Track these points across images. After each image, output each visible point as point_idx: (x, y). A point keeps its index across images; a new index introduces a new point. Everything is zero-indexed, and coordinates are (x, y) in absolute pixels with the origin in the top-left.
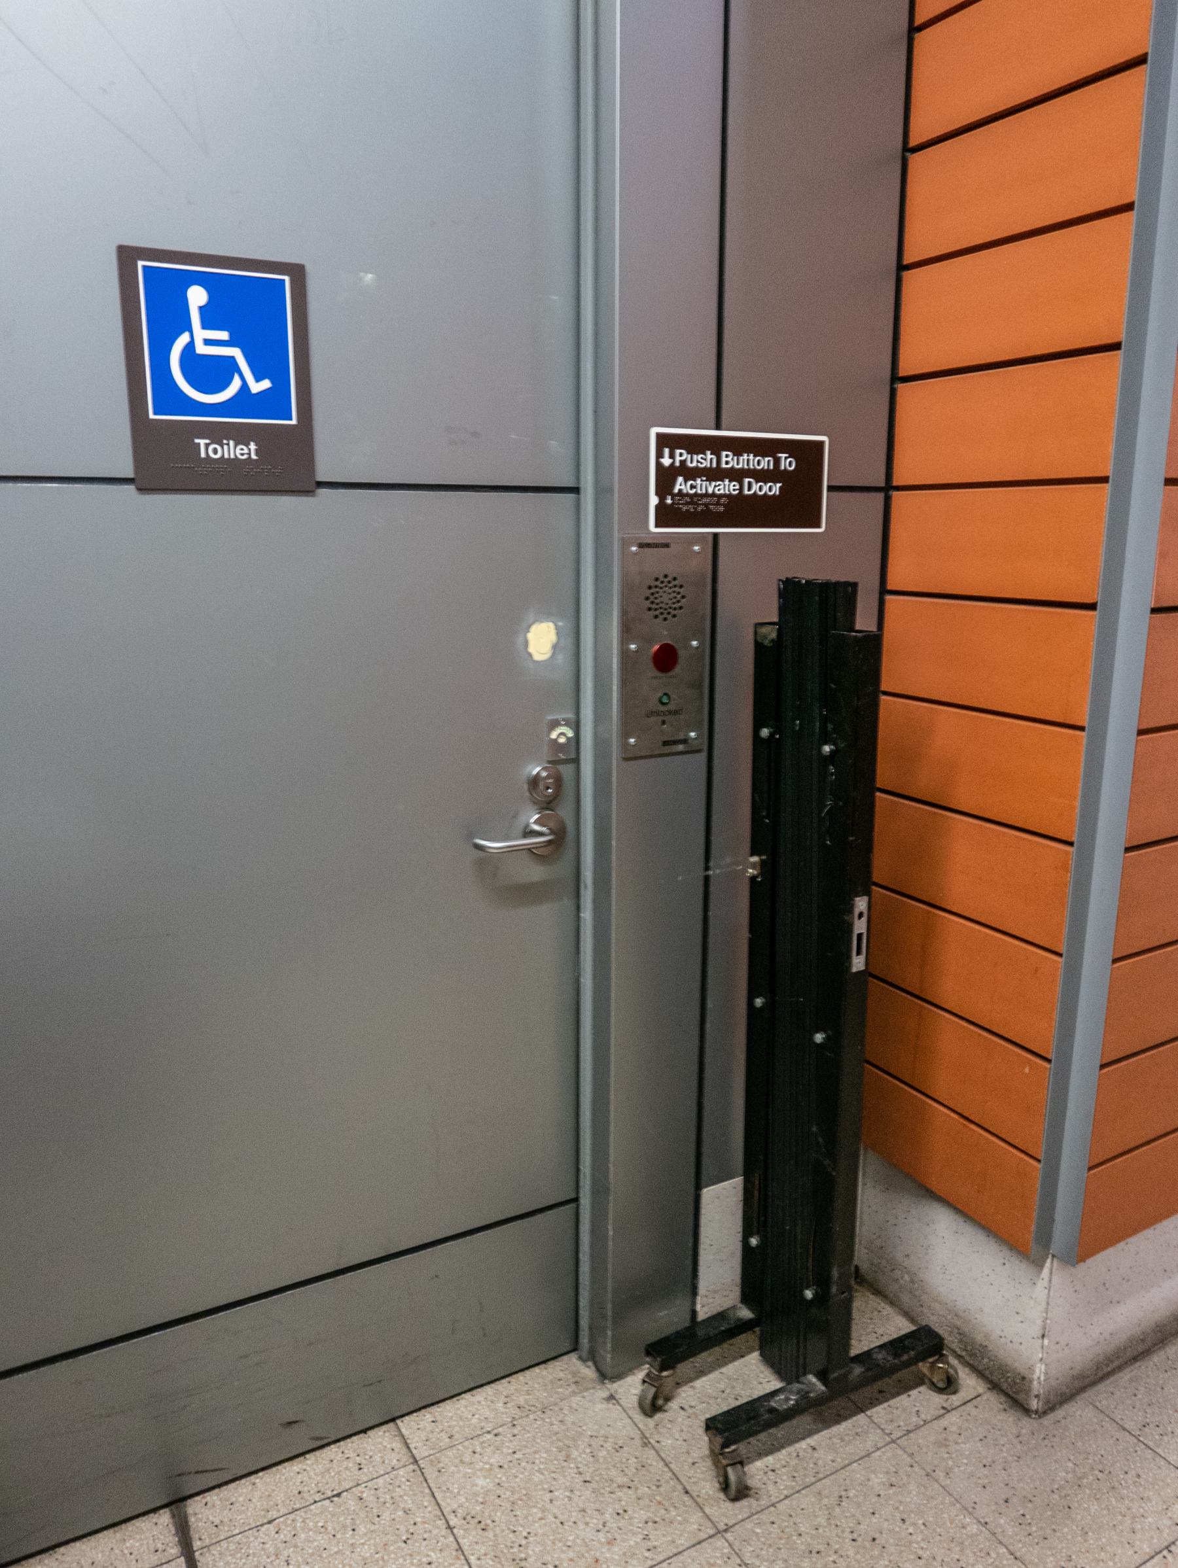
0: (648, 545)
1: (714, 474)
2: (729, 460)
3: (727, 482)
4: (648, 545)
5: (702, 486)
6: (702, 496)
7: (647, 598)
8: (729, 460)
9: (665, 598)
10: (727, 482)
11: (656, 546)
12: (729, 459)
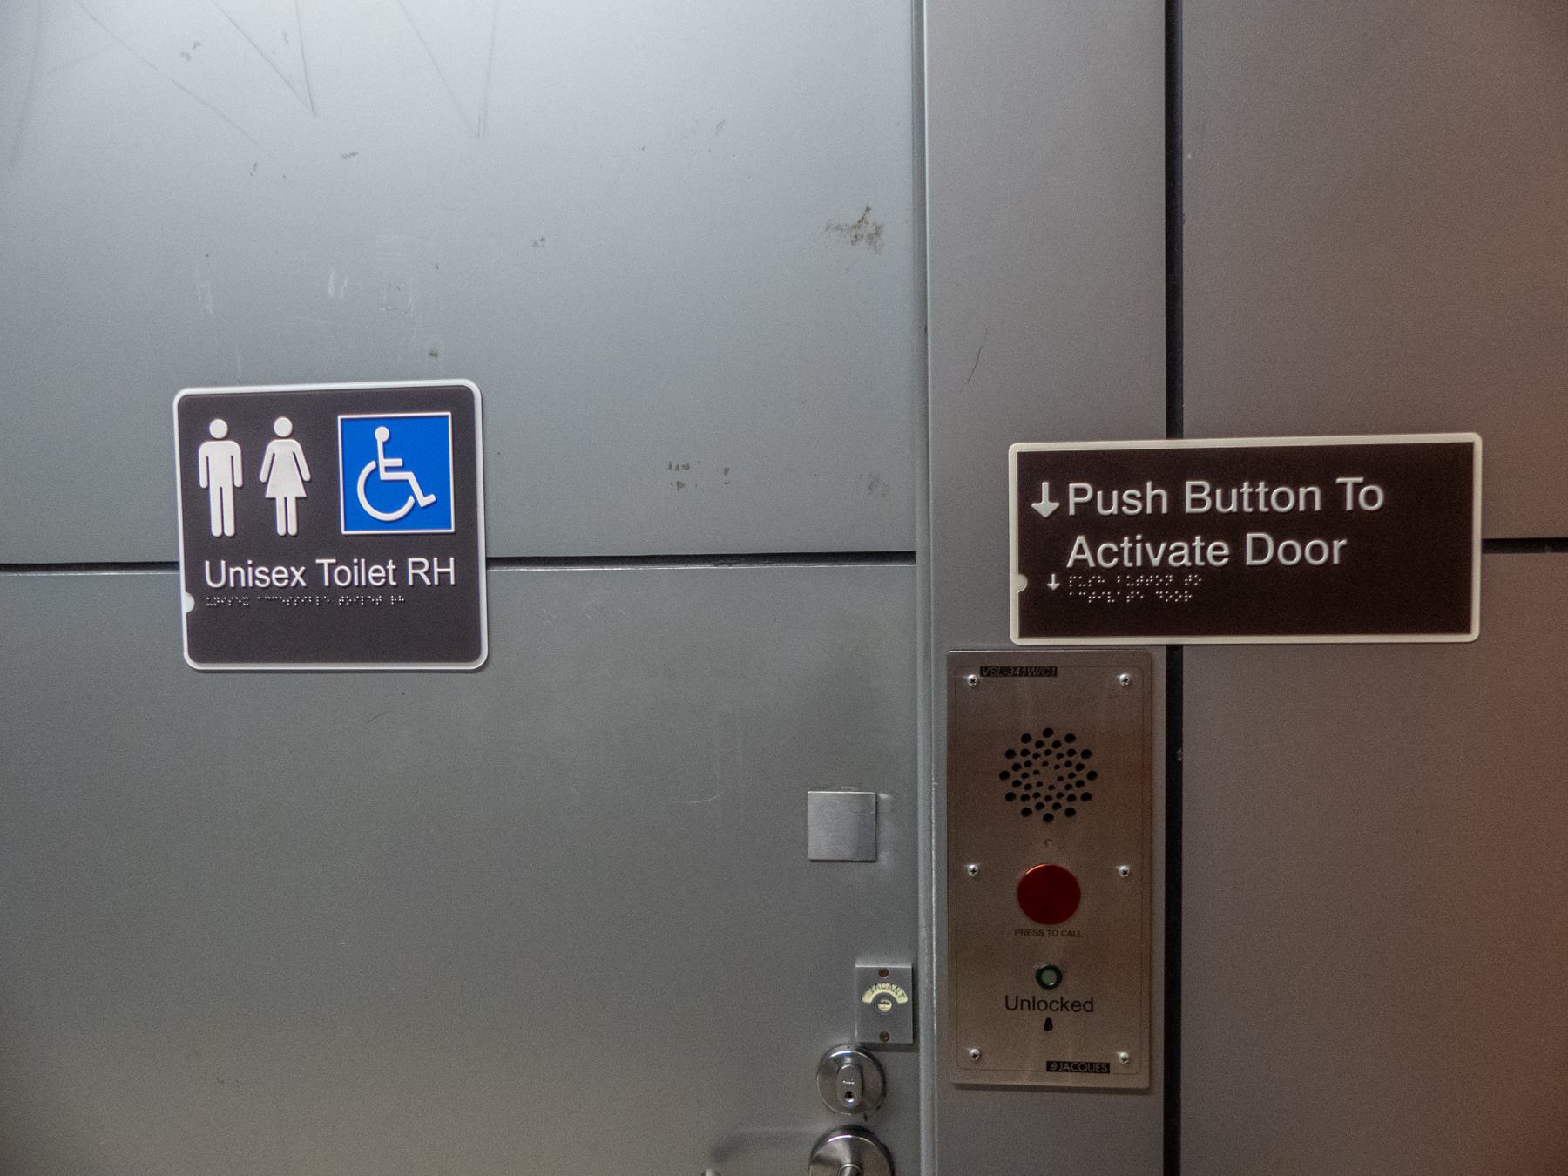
0: (1005, 671)
1: (1169, 525)
2: (1199, 496)
3: (1198, 542)
4: (1005, 671)
6: (1135, 572)
7: (1004, 775)
9: (1049, 776)
10: (1198, 542)
11: (1025, 672)
12: (1204, 495)
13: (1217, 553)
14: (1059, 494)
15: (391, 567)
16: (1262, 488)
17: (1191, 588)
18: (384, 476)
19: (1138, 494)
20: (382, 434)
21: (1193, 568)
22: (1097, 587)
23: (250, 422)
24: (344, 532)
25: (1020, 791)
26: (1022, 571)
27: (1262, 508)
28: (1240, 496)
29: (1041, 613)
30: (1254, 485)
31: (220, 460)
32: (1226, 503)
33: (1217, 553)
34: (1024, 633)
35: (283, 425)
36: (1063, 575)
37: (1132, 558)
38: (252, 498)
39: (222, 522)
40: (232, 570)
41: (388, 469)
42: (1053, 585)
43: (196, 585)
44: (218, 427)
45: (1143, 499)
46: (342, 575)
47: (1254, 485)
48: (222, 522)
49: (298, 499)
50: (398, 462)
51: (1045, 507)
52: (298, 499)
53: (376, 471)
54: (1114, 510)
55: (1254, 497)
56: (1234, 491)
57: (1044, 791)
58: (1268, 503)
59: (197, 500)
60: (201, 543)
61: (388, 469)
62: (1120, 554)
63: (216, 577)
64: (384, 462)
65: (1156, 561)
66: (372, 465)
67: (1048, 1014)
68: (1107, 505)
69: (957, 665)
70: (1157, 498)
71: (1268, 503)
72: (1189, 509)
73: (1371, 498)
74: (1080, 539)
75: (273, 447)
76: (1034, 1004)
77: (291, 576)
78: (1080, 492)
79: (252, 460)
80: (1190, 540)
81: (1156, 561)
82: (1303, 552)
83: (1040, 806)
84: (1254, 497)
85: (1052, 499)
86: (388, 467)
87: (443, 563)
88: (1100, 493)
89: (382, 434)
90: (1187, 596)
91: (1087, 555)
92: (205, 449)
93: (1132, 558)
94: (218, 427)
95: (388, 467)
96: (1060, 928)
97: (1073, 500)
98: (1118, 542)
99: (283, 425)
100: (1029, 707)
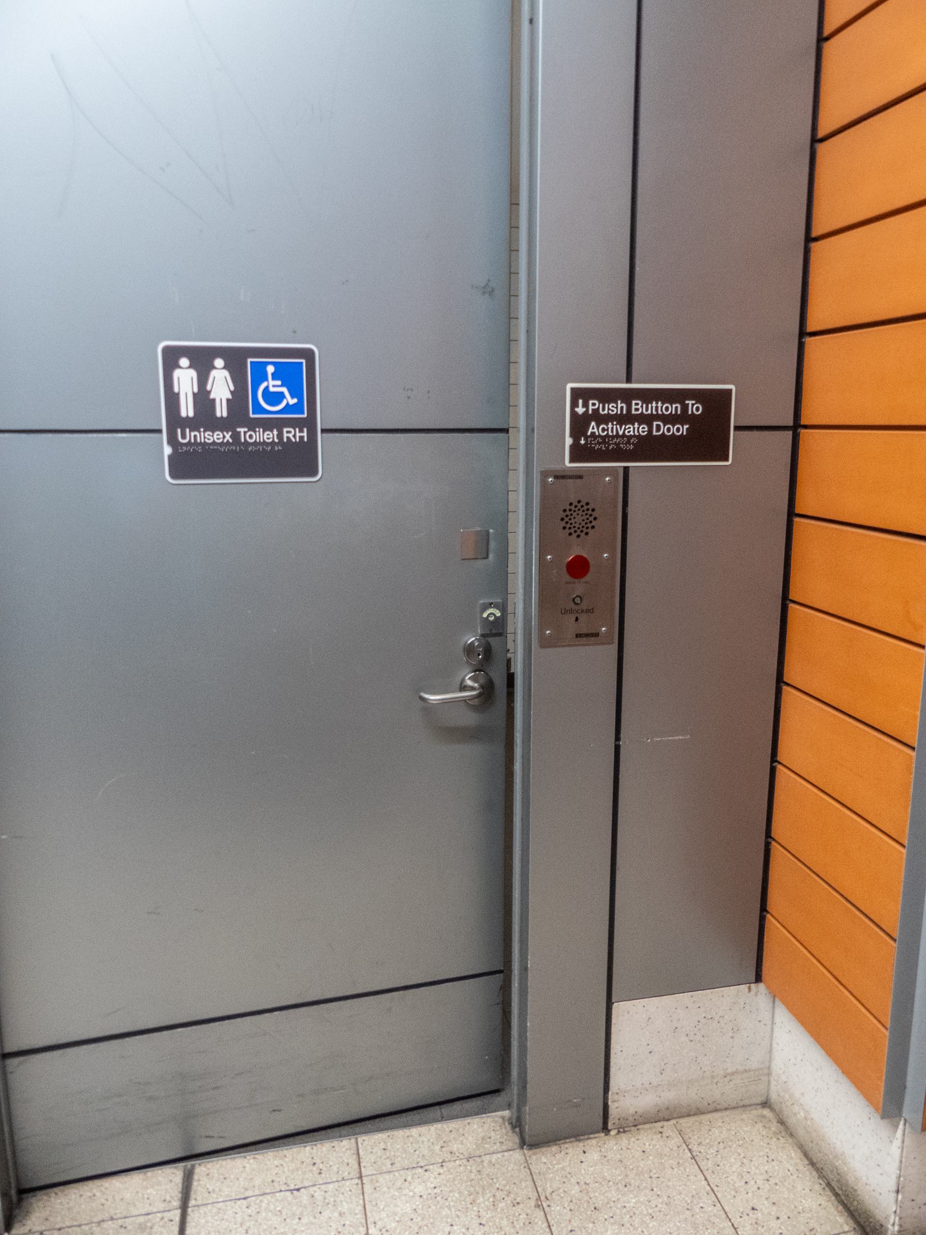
0: (563, 477)
1: (626, 419)
2: (638, 407)
3: (636, 425)
4: (563, 477)
5: (612, 428)
6: (613, 437)
7: (562, 519)
8: (638, 407)
9: (579, 519)
10: (636, 425)
11: (571, 477)
12: (639, 407)
13: (643, 430)
14: (585, 405)
15: (275, 432)
16: (660, 404)
17: (633, 444)
18: (272, 389)
20: (270, 369)
21: (635, 436)
22: (599, 443)
23: (202, 360)
24: (251, 416)
25: (568, 526)
26: (571, 436)
27: (660, 412)
29: (578, 453)
30: (657, 403)
31: (185, 379)
32: (647, 410)
33: (643, 430)
34: (572, 461)
35: (219, 363)
36: (586, 438)
37: (612, 431)
38: (203, 398)
39: (187, 409)
40: (193, 434)
41: (274, 386)
42: (583, 442)
43: (172, 441)
44: (184, 362)
45: (617, 408)
46: (251, 437)
47: (657, 403)
48: (187, 409)
49: (228, 400)
50: (279, 383)
51: (580, 410)
52: (228, 400)
53: (267, 387)
54: (606, 412)
55: (657, 407)
57: (577, 525)
59: (172, 399)
60: (175, 420)
61: (274, 386)
62: (607, 430)
63: (184, 437)
64: (272, 383)
65: (621, 433)
66: (264, 385)
67: (578, 615)
68: (603, 410)
69: (545, 474)
70: (622, 408)
72: (633, 412)
73: (697, 409)
74: (593, 423)
75: (214, 373)
76: (571, 611)
77: (224, 437)
78: (594, 404)
79: (203, 380)
80: (633, 425)
81: (621, 433)
82: (674, 430)
83: (575, 532)
84: (657, 407)
85: (583, 406)
86: (274, 385)
87: (301, 431)
89: (270, 369)
90: (632, 447)
91: (596, 430)
92: (177, 373)
93: (612, 431)
94: (184, 362)
95: (274, 385)
96: (583, 580)
97: (591, 407)
98: (607, 425)
99: (219, 363)
100: (572, 492)
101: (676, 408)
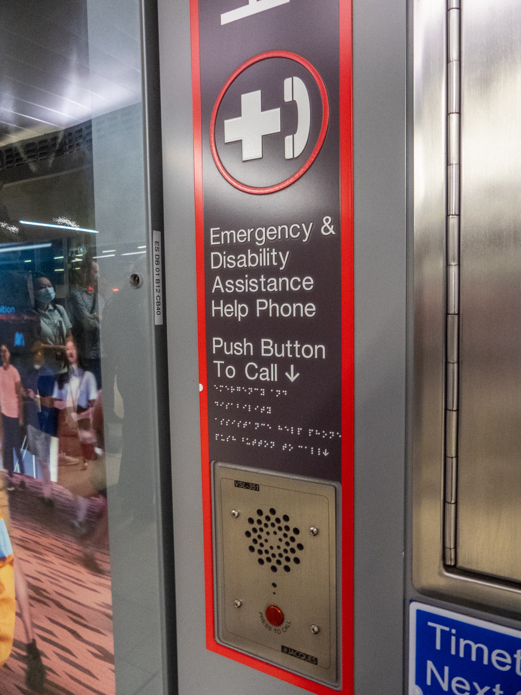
16: (297, 345)
19: (241, 345)
28: (286, 348)
30: (293, 343)
32: (280, 352)
45: (242, 348)
47: (293, 343)
54: (231, 352)
55: (293, 349)
56: (283, 345)
58: (300, 353)
70: (248, 347)
71: (300, 353)
78: (218, 343)
84: (293, 349)
88: (225, 343)
101: (320, 350)
